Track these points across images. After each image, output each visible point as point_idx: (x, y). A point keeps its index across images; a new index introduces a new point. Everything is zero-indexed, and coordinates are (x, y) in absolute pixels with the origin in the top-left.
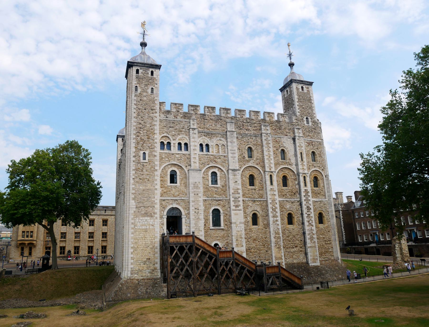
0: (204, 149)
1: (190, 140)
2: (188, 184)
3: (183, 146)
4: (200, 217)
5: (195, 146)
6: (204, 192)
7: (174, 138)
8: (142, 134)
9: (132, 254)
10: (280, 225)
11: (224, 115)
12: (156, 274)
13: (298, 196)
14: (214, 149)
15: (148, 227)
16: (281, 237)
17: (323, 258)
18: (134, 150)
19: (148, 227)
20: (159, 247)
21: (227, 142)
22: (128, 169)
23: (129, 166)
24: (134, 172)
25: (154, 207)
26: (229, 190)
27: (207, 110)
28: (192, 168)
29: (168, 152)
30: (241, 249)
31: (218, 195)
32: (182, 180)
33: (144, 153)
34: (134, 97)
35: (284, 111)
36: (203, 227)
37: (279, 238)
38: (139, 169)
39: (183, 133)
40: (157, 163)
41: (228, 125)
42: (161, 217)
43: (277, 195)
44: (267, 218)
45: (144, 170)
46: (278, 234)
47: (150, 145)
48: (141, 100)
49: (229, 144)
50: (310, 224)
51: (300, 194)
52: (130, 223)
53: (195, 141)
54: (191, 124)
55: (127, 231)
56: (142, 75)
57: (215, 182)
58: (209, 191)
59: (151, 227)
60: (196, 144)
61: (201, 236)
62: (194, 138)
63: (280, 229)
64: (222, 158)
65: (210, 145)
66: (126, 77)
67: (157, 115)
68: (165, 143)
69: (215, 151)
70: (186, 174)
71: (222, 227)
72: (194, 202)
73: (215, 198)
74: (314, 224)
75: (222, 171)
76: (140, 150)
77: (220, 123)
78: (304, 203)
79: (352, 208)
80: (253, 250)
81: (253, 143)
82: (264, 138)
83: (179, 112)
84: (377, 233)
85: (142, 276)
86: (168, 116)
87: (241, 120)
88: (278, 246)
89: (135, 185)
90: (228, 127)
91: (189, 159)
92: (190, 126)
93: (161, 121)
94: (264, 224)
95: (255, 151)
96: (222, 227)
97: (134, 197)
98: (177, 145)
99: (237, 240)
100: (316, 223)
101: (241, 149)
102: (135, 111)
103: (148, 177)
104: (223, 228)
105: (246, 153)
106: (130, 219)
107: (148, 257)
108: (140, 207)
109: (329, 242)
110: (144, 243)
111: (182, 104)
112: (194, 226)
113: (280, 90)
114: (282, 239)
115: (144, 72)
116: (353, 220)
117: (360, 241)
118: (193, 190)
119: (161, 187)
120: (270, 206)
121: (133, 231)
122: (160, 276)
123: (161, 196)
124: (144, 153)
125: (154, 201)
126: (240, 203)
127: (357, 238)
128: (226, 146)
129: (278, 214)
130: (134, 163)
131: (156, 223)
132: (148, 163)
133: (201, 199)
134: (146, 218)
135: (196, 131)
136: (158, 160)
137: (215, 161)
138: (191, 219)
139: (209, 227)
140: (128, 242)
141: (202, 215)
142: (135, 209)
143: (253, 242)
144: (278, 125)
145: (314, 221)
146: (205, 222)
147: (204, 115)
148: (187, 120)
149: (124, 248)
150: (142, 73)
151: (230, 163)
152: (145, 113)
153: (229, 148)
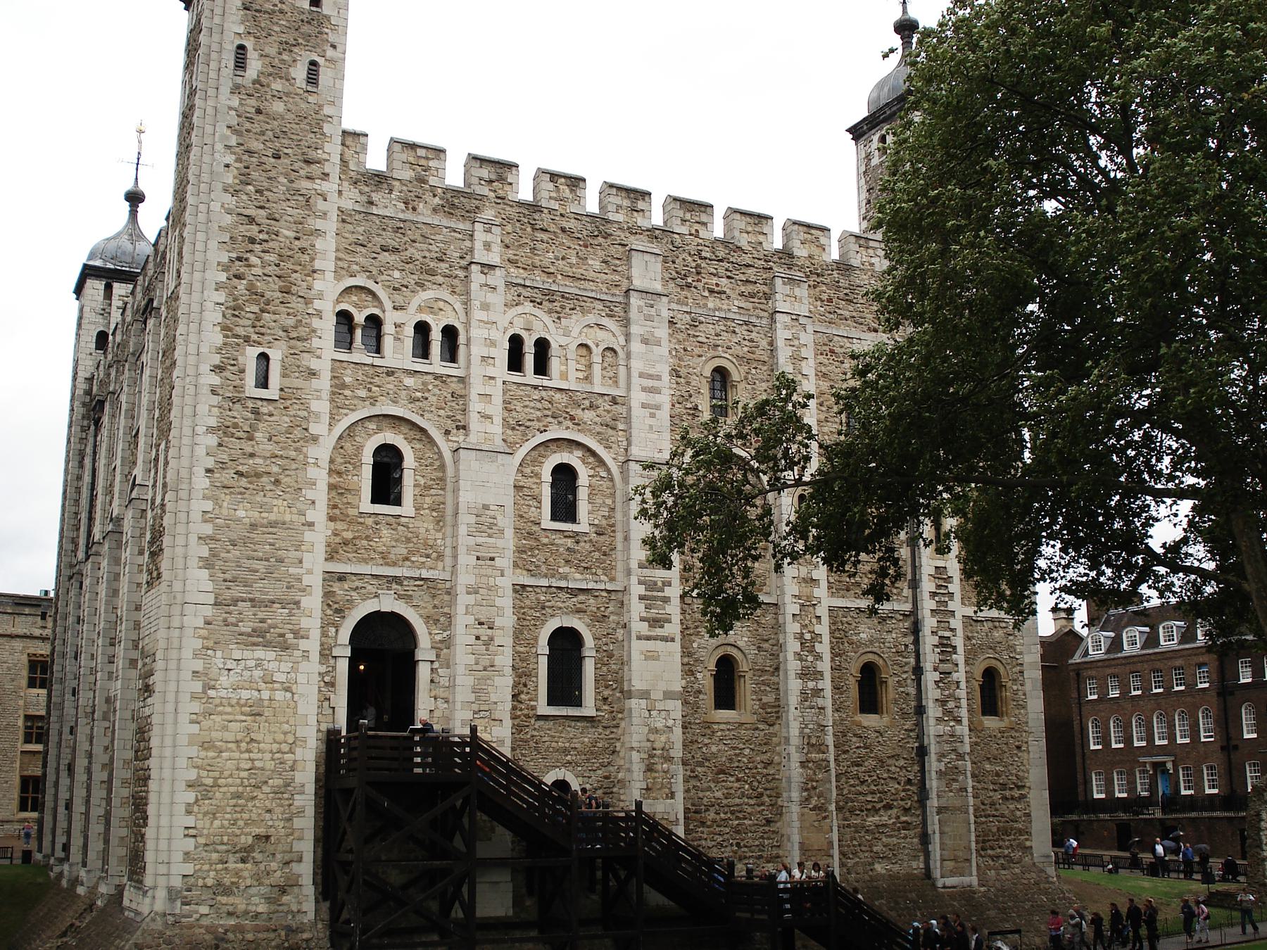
0: (529, 361)
2: (449, 511)
3: (436, 336)
4: (499, 661)
5: (493, 344)
6: (520, 551)
7: (399, 299)
9: (189, 812)
11: (620, 217)
12: (295, 909)
13: (907, 592)
14: (572, 365)
15: (266, 695)
16: (832, 765)
17: (992, 857)
18: (218, 339)
19: (266, 695)
20: (310, 788)
21: (628, 336)
22: (187, 422)
24: (212, 440)
25: (297, 603)
26: (627, 549)
27: (551, 186)
28: (473, 439)
29: (369, 361)
30: (670, 810)
31: (578, 567)
33: (264, 357)
35: (865, 224)
36: (509, 706)
37: (823, 766)
38: (236, 426)
39: (440, 279)
40: (321, 406)
41: (637, 259)
42: (326, 654)
43: (824, 584)
44: (774, 679)
46: (821, 747)
47: (291, 321)
48: (259, 111)
49: (636, 346)
50: (951, 716)
51: (915, 584)
53: (490, 322)
54: (478, 245)
55: (170, 707)
57: (564, 508)
58: (540, 546)
59: (279, 695)
61: (502, 742)
62: (485, 307)
64: (604, 405)
65: (554, 345)
67: (330, 187)
68: (359, 318)
69: (573, 375)
70: (442, 467)
71: (588, 709)
72: (477, 593)
73: (565, 578)
74: (964, 713)
75: (601, 462)
76: (247, 339)
77: (601, 253)
78: (929, 623)
79: (1077, 659)
80: (711, 815)
81: (737, 350)
82: (782, 334)
83: (422, 180)
84: (1169, 766)
85: (230, 914)
88: (814, 802)
89: (216, 500)
90: (635, 272)
92: (471, 250)
93: (344, 217)
94: (763, 706)
95: (741, 386)
96: (588, 709)
97: (206, 553)
98: (409, 331)
99: (650, 769)
101: (683, 372)
102: (230, 159)
103: (275, 469)
104: (593, 713)
105: (705, 390)
106: (187, 654)
107: (261, 831)
108: (235, 602)
109: (1016, 793)
110: (249, 765)
111: (443, 151)
112: (472, 697)
113: (849, 130)
114: (833, 772)
116: (1075, 709)
117: (1096, 796)
120: (793, 628)
121: (196, 707)
122: (311, 916)
123: (330, 557)
124: (264, 357)
125: (300, 580)
126: (669, 609)
127: (1087, 783)
128: (621, 353)
129: (825, 666)
130: (216, 400)
131: (302, 678)
133: (506, 583)
134: (260, 653)
135: (497, 278)
136: (326, 395)
137: (572, 418)
138: (460, 669)
139: (534, 708)
141: (508, 651)
142: (209, 611)
144: (843, 283)
145: (964, 703)
146: (514, 687)
147: (534, 207)
148: (461, 226)
149: (153, 785)
151: (634, 432)
152: (272, 174)
153: (637, 365)
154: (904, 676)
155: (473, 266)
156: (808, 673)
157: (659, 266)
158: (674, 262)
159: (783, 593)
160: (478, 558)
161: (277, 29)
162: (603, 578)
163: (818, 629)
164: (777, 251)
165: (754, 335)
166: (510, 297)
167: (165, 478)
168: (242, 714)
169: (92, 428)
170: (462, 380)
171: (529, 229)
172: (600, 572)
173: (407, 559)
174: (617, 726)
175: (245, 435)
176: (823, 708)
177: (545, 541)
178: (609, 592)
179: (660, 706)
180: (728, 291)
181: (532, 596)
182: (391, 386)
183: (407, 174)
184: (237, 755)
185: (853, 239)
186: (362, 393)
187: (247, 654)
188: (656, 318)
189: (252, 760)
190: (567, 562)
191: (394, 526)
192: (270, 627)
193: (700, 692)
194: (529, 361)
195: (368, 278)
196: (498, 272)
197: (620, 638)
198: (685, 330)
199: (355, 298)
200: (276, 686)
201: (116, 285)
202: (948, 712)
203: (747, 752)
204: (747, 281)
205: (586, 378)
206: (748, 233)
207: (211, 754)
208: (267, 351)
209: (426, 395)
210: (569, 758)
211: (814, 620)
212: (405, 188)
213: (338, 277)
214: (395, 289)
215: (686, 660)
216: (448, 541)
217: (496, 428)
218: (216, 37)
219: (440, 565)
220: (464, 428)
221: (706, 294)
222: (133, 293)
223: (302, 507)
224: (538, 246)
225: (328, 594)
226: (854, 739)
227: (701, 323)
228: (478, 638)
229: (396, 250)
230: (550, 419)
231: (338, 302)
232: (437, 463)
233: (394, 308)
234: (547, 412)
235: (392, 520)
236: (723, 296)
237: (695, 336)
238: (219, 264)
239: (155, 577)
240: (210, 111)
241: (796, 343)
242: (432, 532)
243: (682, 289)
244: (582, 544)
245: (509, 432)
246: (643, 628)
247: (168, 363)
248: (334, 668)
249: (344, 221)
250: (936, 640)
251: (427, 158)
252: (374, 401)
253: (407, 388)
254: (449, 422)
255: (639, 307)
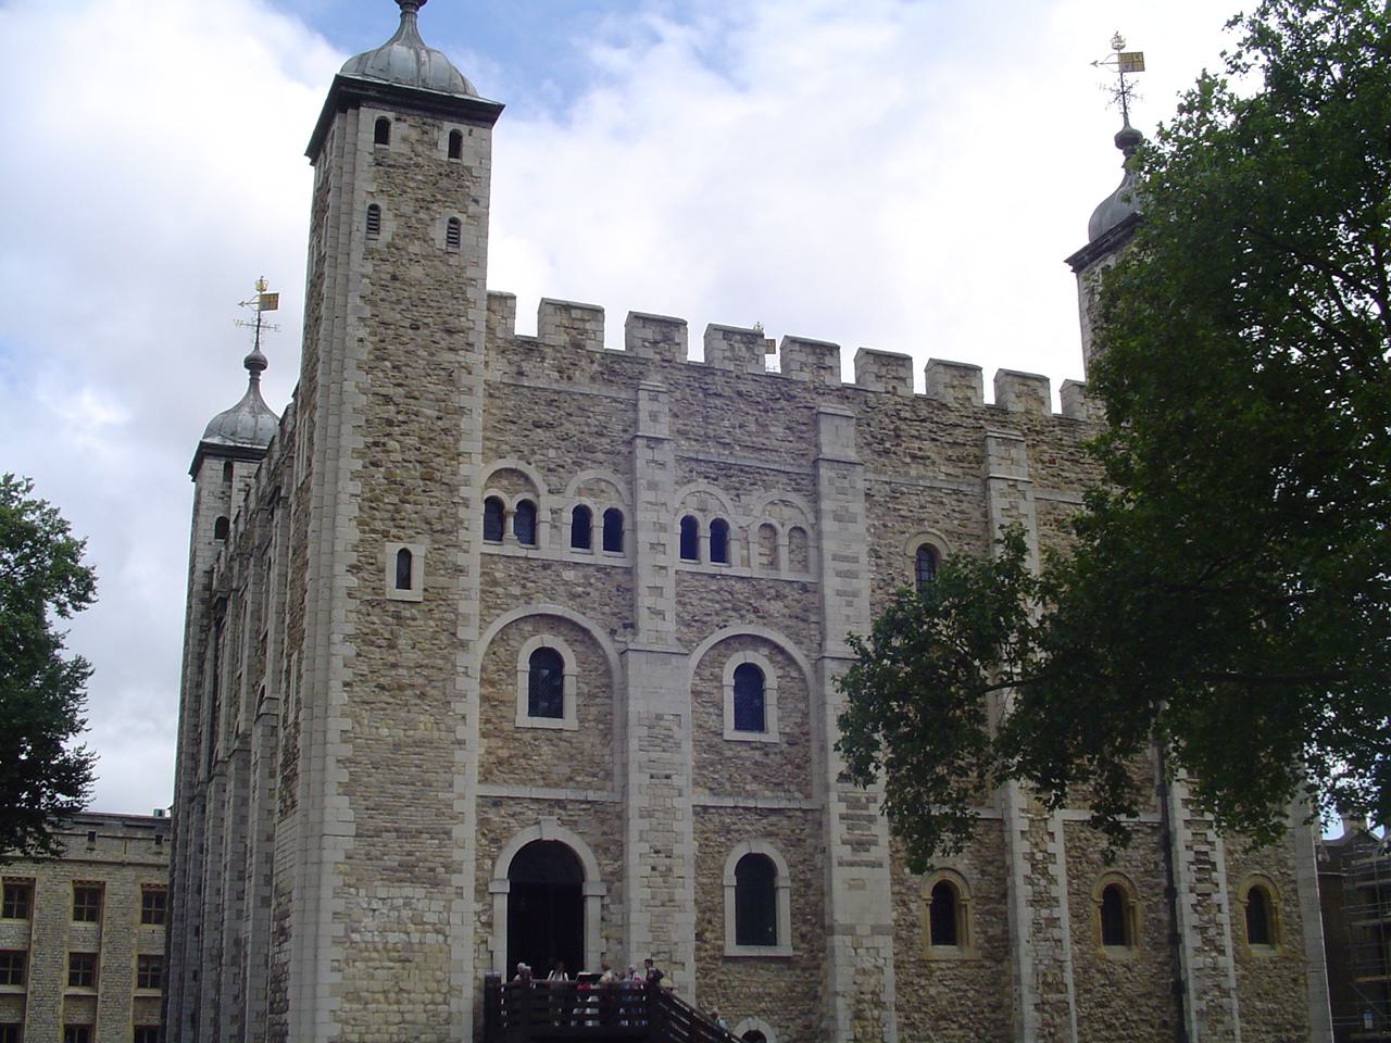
0: (705, 546)
1: (633, 493)
2: (617, 724)
4: (679, 894)
5: (663, 528)
6: (700, 766)
7: (554, 480)
8: (397, 457)
10: (1067, 944)
11: (806, 376)
13: (1155, 800)
14: (755, 549)
15: (415, 938)
19: (415, 938)
21: (818, 513)
23: (322, 616)
24: (350, 649)
25: (448, 833)
26: (824, 761)
28: (643, 639)
29: (523, 553)
31: (767, 783)
32: (588, 699)
33: (405, 556)
34: (360, 266)
36: (692, 944)
37: (1062, 1009)
38: (375, 632)
39: (600, 456)
40: (470, 607)
42: (482, 891)
44: (1002, 907)
45: (401, 642)
46: (1059, 987)
47: (434, 512)
49: (828, 525)
52: (326, 916)
53: (661, 503)
54: (643, 416)
56: (405, 149)
57: (750, 714)
58: (724, 760)
59: (431, 938)
60: (665, 518)
61: (684, 988)
63: (1069, 966)
65: (733, 527)
66: (316, 150)
67: (475, 359)
68: (511, 504)
69: (756, 560)
70: (608, 673)
71: (784, 947)
73: (753, 795)
74: (1227, 942)
75: (791, 660)
76: (386, 534)
81: (945, 524)
83: (581, 347)
86: (526, 366)
87: (890, 408)
90: (824, 438)
91: (627, 592)
92: (635, 422)
93: (492, 391)
94: (990, 940)
96: (784, 947)
98: (568, 517)
99: (858, 1016)
100: (1236, 938)
101: (883, 551)
102: (363, 333)
103: (420, 681)
106: (326, 893)
108: (378, 833)
110: (398, 1018)
115: (414, 135)
118: (644, 756)
119: (484, 735)
120: (1021, 847)
121: (338, 952)
123: (486, 777)
124: (405, 556)
125: (450, 806)
128: (810, 533)
129: (1061, 890)
131: (455, 919)
132: (422, 607)
134: (408, 891)
135: (666, 453)
137: (756, 610)
138: (635, 905)
140: (315, 1010)
141: (690, 883)
143: (936, 1029)
144: (1067, 440)
145: (1227, 929)
146: (698, 924)
148: (623, 395)
150: (405, 139)
151: (829, 625)
152: (410, 347)
153: (829, 546)
154: (1155, 900)
155: (638, 441)
156: (1040, 900)
157: (851, 431)
158: (869, 425)
159: (1009, 807)
160: (652, 777)
161: (412, 185)
162: (797, 794)
163: (1051, 847)
164: (989, 407)
165: (964, 506)
166: (680, 473)
167: (298, 693)
168: (391, 960)
169: (213, 629)
170: (629, 571)
171: (701, 395)
172: (793, 788)
173: (571, 779)
174: (818, 967)
175: (384, 643)
176: (1060, 941)
177: (729, 753)
178: (804, 811)
179: (867, 943)
180: (933, 456)
181: (716, 819)
182: (548, 581)
183: (562, 339)
184: (385, 1007)
185: (1077, 390)
186: (516, 590)
187: (394, 892)
188: (850, 491)
189: (402, 1013)
190: (755, 777)
191: (556, 741)
192: (419, 860)
193: (914, 925)
194: (705, 546)
195: (519, 458)
196: (667, 446)
197: (819, 865)
198: (885, 503)
199: (505, 482)
200: (427, 927)
201: (236, 465)
202: (1207, 941)
203: (971, 994)
204: (955, 443)
205: (771, 563)
206: (953, 387)
207: (355, 1006)
208: (409, 547)
209: (589, 589)
210: (763, 1005)
211: (1046, 838)
212: (559, 355)
213: (486, 460)
214: (550, 470)
215: (897, 888)
216: (617, 758)
217: (670, 625)
218: (345, 197)
219: (609, 785)
220: (632, 626)
221: (908, 460)
222: (257, 476)
223: (450, 722)
224: (713, 413)
225: (483, 822)
226: (1098, 976)
227: (903, 493)
228: (654, 869)
229: (549, 426)
230: (730, 613)
231: (487, 487)
232: (603, 668)
233: (550, 492)
234: (729, 605)
235: (553, 735)
236: (928, 462)
237: (895, 509)
238: (354, 450)
239: (289, 807)
240: (340, 279)
241: (1014, 513)
242: (600, 747)
243: (880, 455)
244: (772, 756)
245: (685, 630)
246: (845, 852)
247: (299, 562)
248: (491, 906)
249: (491, 395)
250: (1190, 856)
251: (583, 320)
252: (528, 598)
253: (566, 583)
254: (615, 619)
255: (831, 480)
